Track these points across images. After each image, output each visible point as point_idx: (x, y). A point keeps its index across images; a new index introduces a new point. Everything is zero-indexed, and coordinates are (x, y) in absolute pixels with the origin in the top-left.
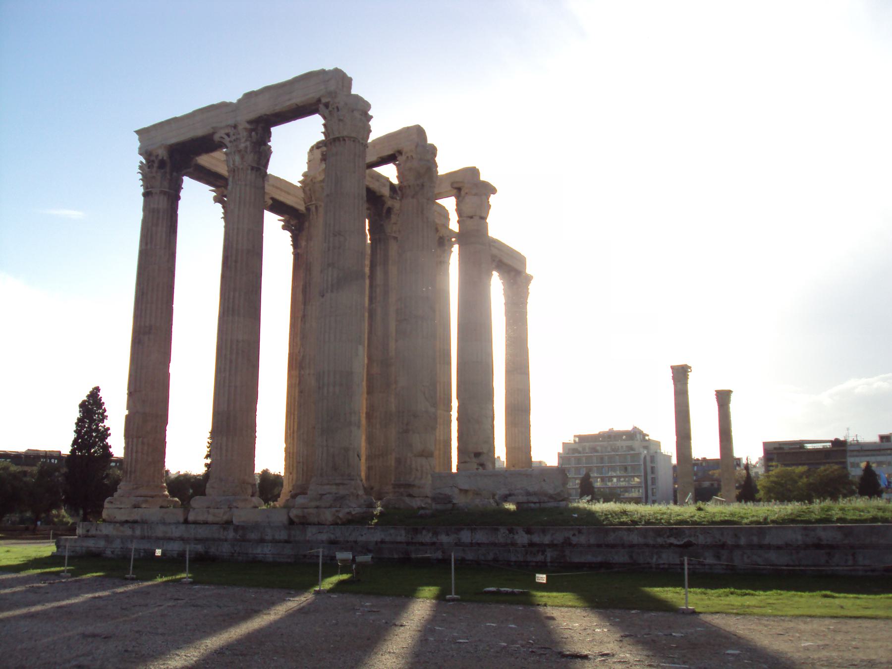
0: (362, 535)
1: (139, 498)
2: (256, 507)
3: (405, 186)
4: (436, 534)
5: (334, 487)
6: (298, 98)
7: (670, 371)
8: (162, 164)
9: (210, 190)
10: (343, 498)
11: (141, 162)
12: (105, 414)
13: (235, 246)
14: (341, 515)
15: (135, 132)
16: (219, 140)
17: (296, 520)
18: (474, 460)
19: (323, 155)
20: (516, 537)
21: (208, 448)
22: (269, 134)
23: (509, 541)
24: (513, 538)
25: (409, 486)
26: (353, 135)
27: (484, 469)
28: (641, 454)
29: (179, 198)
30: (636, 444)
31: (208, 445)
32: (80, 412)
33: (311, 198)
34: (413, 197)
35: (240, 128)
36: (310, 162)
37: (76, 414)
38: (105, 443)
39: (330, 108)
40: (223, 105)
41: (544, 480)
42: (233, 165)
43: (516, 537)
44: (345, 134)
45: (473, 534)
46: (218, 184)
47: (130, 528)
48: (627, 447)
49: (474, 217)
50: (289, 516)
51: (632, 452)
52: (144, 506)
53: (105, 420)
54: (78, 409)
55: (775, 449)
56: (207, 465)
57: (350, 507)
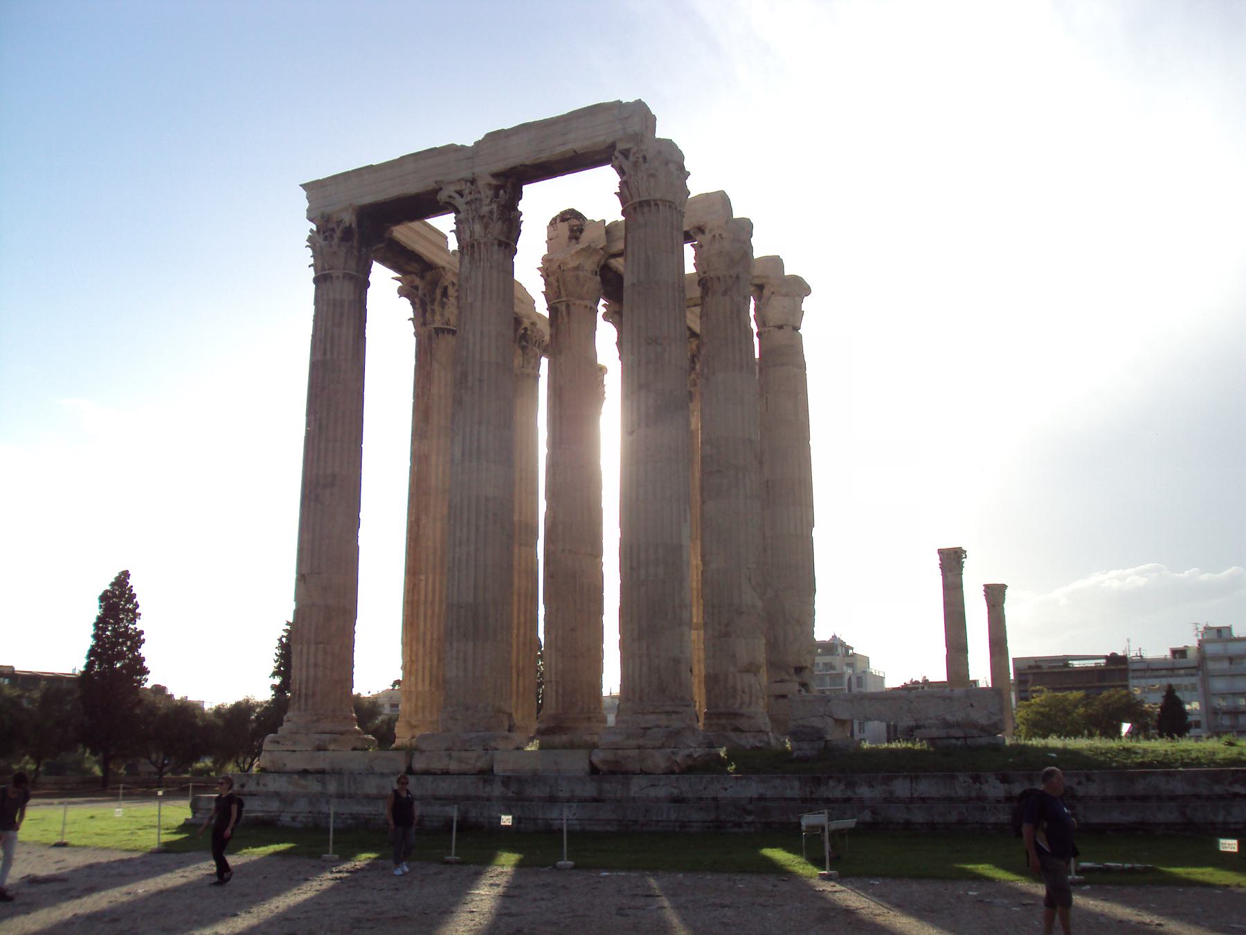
0: (726, 789)
1: (327, 737)
2: (518, 748)
3: (711, 278)
4: (850, 784)
5: (663, 717)
6: (578, 142)
7: (938, 557)
8: (347, 234)
9: (393, 278)
10: (677, 733)
11: (311, 231)
12: (137, 611)
13: (478, 357)
14: (679, 759)
15: (300, 185)
16: (447, 200)
17: (600, 766)
18: (795, 678)
19: (572, 230)
20: (985, 787)
21: (276, 662)
22: (518, 195)
23: (973, 794)
24: (981, 789)
25: (735, 715)
26: (670, 198)
27: (807, 690)
28: (845, 673)
29: (368, 284)
30: (837, 661)
31: (276, 658)
32: (101, 607)
33: (560, 293)
34: (725, 293)
35: (481, 183)
36: (550, 240)
37: (94, 610)
38: (136, 654)
39: (632, 158)
40: (452, 149)
41: (972, 705)
42: (471, 237)
43: (985, 787)
44: (658, 195)
45: (914, 785)
46: (410, 269)
47: (318, 781)
48: (825, 664)
49: (784, 327)
50: (591, 762)
51: (832, 672)
52: (332, 747)
53: (137, 620)
54: (97, 603)
55: (1030, 667)
56: (273, 687)
57: (689, 747)
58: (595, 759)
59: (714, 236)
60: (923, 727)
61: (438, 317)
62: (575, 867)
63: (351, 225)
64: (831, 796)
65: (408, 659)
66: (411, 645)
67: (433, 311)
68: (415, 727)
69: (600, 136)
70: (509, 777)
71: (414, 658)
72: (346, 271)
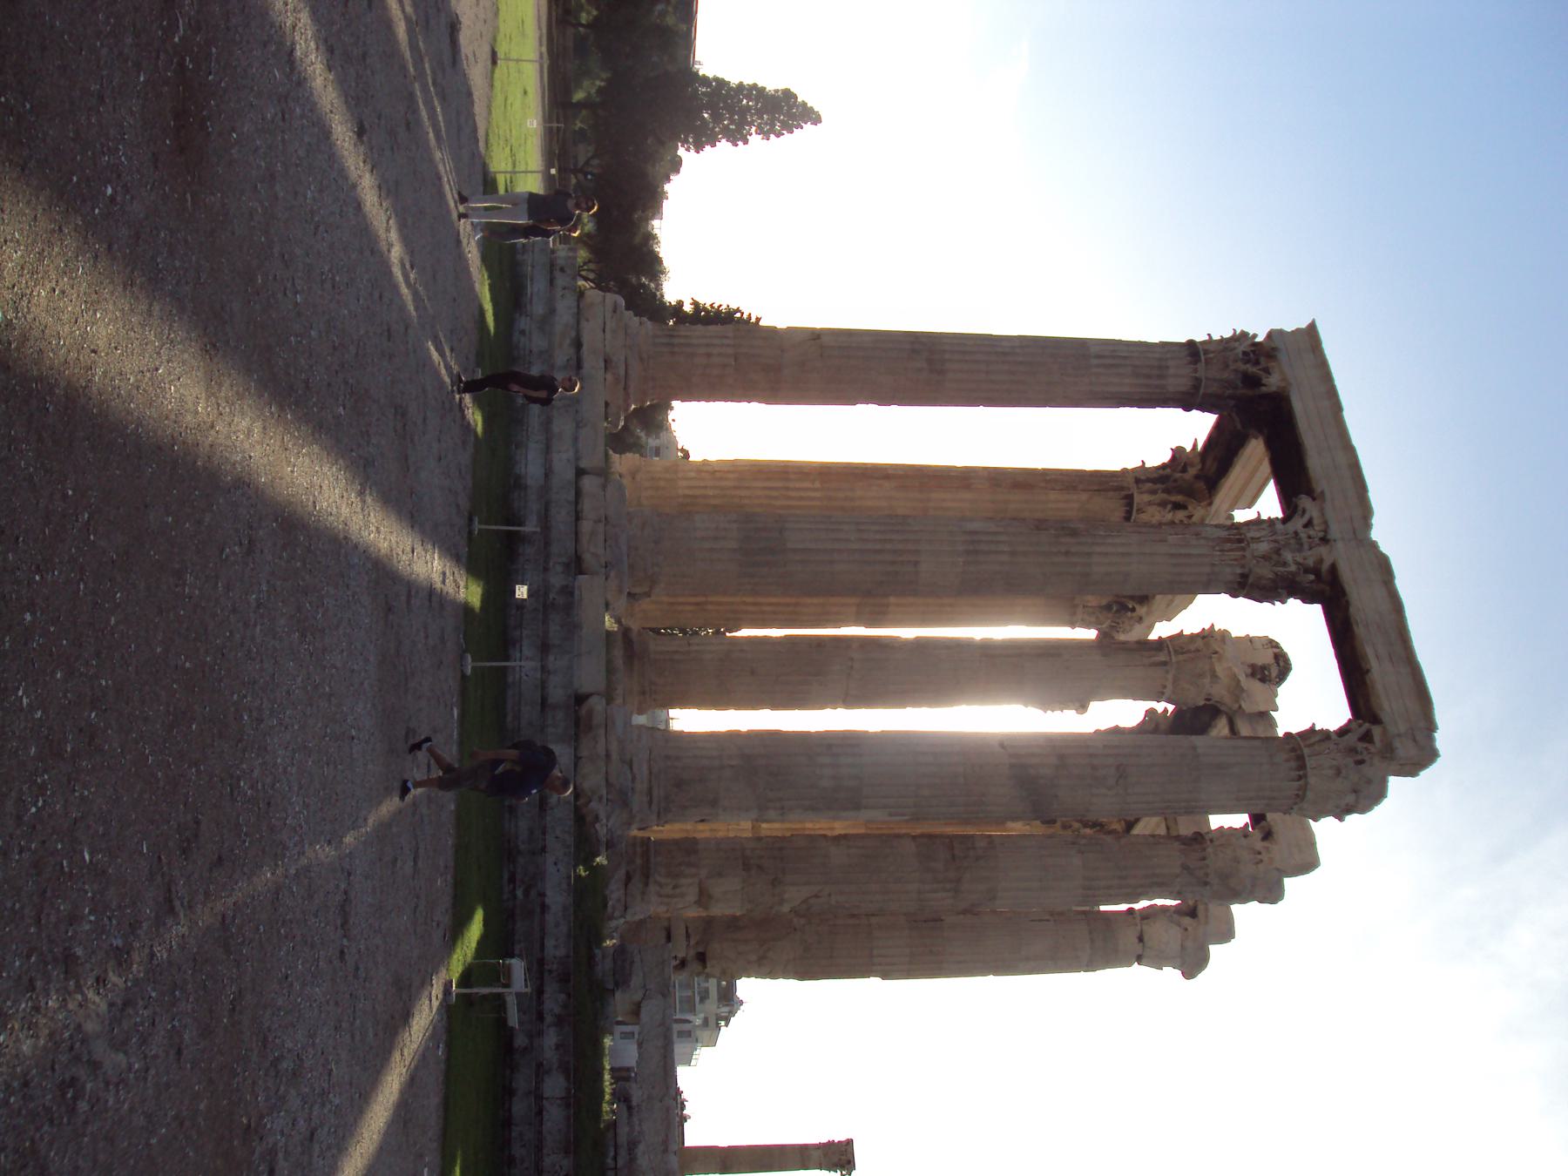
0: (555, 864)
1: (622, 372)
2: (607, 605)
3: (1204, 850)
4: (560, 1021)
6: (1380, 673)
7: (843, 1138)
8: (1252, 381)
9: (1196, 440)
10: (625, 804)
11: (1255, 336)
12: (772, 136)
13: (1098, 549)
14: (593, 805)
16: (1300, 508)
18: (692, 953)
19: (1264, 668)
21: (711, 305)
22: (1308, 599)
25: (646, 876)
26: (1309, 794)
27: (676, 968)
28: (695, 1015)
29: (1187, 408)
30: (712, 1005)
31: (716, 306)
32: (777, 91)
33: (1183, 653)
34: (1185, 867)
35: (1323, 550)
36: (1250, 640)
37: (771, 84)
38: (720, 136)
39: (1361, 746)
40: (1366, 512)
42: (1252, 538)
44: (1312, 780)
45: (559, 1102)
46: (1209, 462)
47: (568, 360)
48: (707, 991)
49: (1141, 944)
51: (697, 999)
52: (609, 377)
53: (761, 136)
54: (781, 87)
56: (680, 303)
58: (593, 700)
59: (1260, 853)
60: (630, 1115)
61: (1147, 497)
62: (464, 676)
63: (1264, 385)
64: (546, 996)
65: (716, 469)
66: (732, 472)
67: (1153, 492)
68: (633, 478)
69: (1390, 704)
70: (572, 594)
71: (718, 475)
72: (1204, 381)
